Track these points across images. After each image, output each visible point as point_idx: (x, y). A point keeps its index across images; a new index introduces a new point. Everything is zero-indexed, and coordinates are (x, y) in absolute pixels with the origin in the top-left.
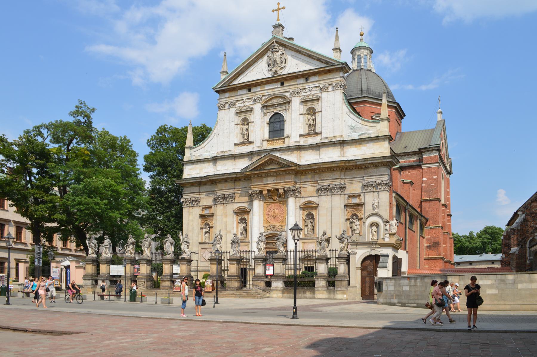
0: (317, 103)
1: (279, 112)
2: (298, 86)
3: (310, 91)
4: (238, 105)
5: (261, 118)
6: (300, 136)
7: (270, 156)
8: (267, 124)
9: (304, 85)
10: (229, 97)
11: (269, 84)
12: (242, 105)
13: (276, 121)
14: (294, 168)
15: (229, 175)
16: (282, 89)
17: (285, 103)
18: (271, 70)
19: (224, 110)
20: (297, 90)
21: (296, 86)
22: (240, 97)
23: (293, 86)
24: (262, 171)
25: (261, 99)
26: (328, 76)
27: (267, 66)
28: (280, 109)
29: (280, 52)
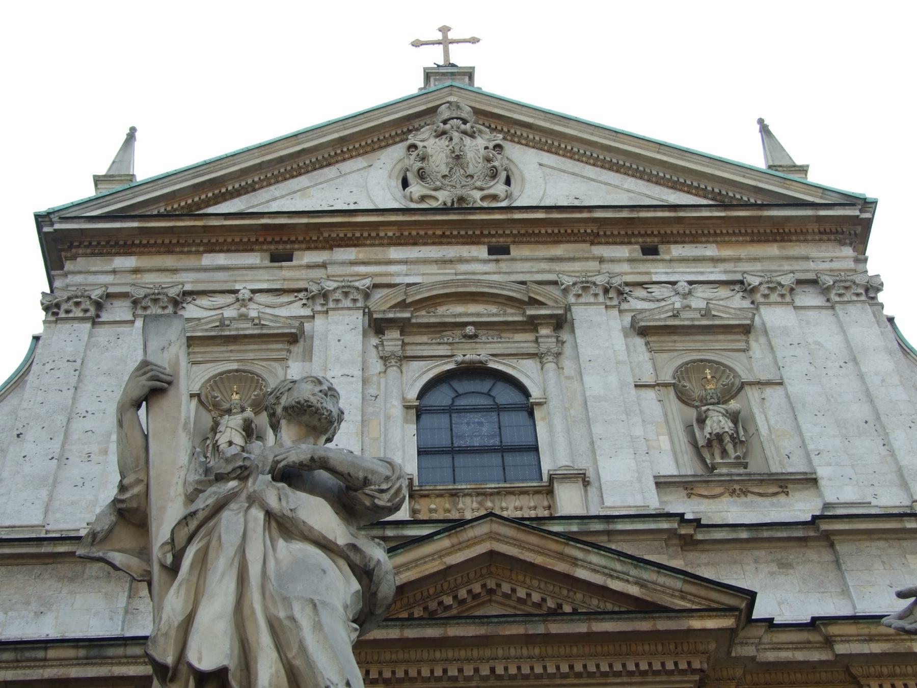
0: (742, 345)
1: (492, 365)
2: (606, 267)
3: (685, 296)
4: (191, 311)
5: (365, 381)
6: (662, 484)
7: (492, 536)
8: (408, 408)
9: (642, 268)
10: (136, 271)
11: (415, 244)
12: (230, 313)
13: (463, 402)
14: (711, 624)
15: (88, 661)
16: (504, 266)
17: (532, 324)
18: (423, 198)
19: (88, 325)
20: (601, 280)
21: (593, 265)
22: (220, 276)
23: (577, 266)
24: (431, 632)
25: (367, 296)
26: (773, 250)
27: (397, 184)
28: (498, 348)
29: (480, 142)
